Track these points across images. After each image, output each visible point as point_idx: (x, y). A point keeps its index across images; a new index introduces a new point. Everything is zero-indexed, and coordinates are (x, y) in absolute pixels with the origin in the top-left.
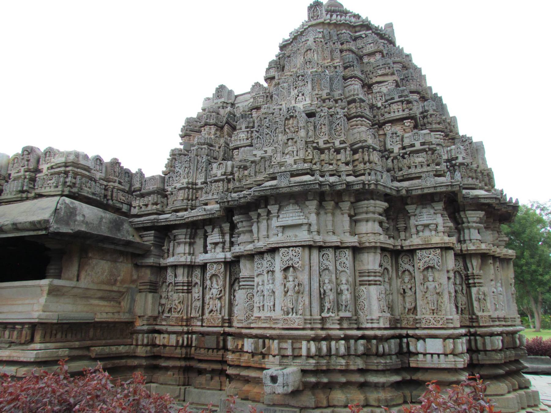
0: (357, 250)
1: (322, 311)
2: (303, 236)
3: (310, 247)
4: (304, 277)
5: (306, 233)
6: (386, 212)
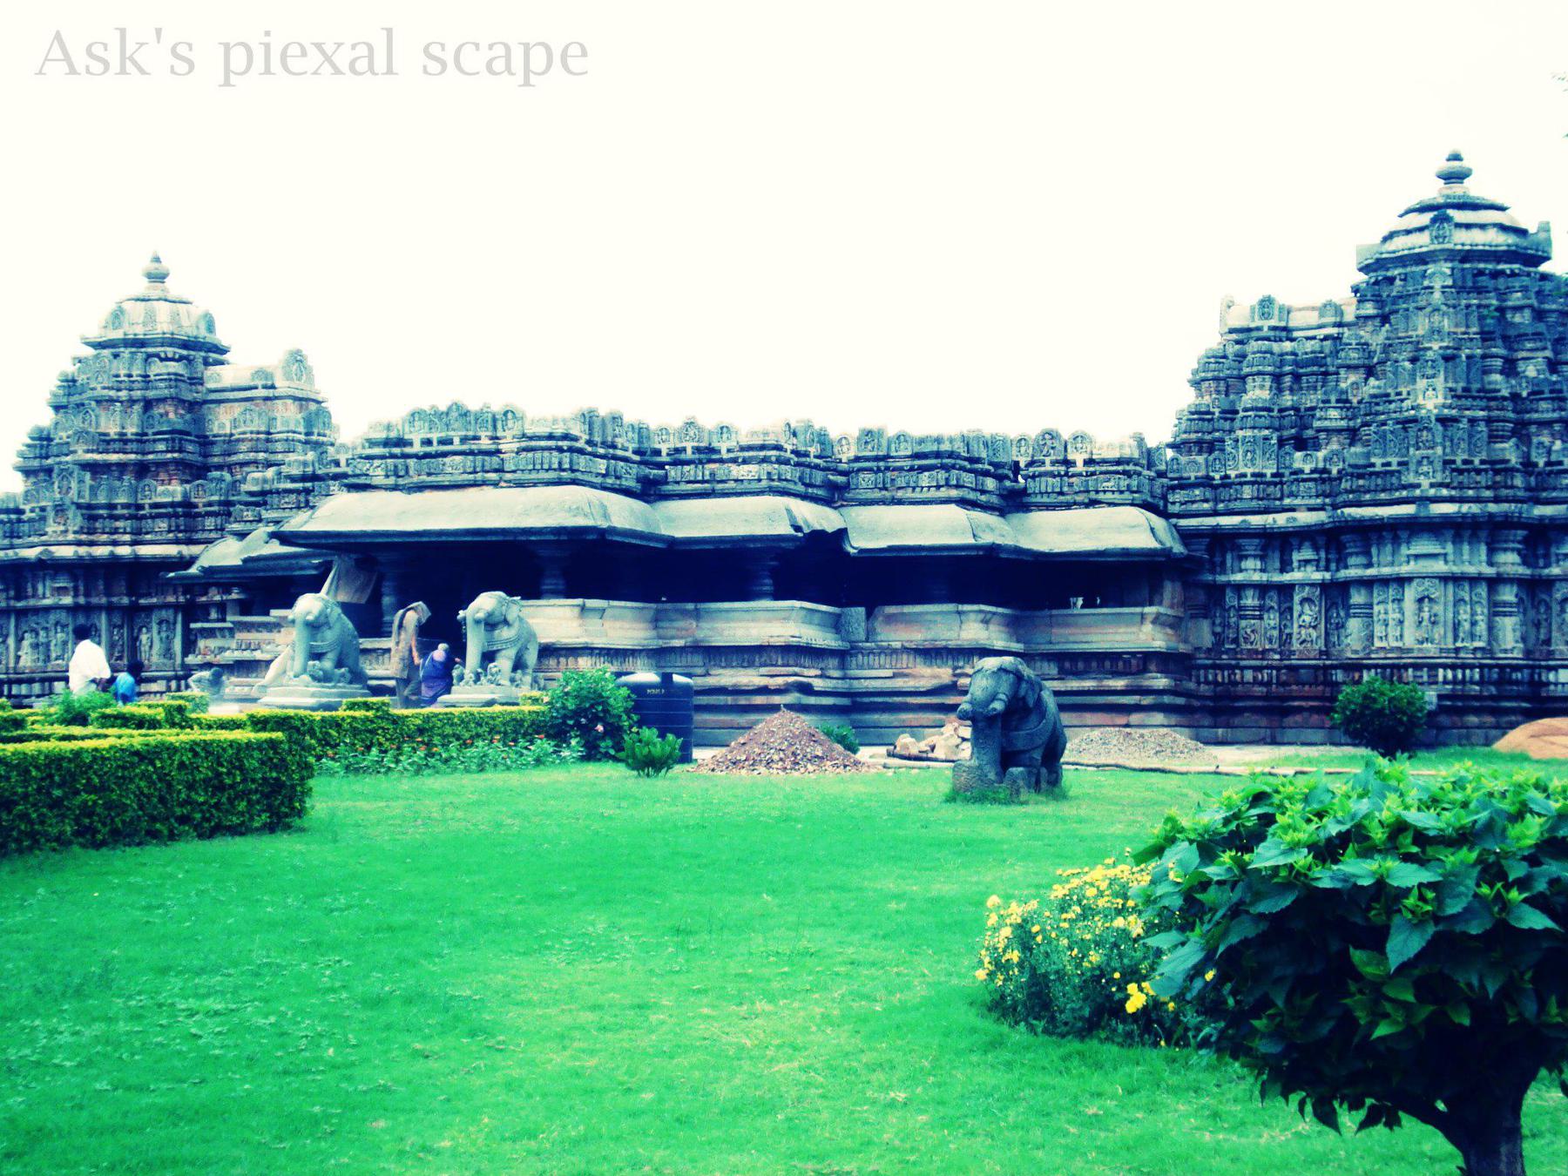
0: (1494, 583)
1: (1455, 640)
2: (1439, 567)
3: (1445, 579)
4: (1438, 609)
5: (1441, 563)
6: (1525, 541)
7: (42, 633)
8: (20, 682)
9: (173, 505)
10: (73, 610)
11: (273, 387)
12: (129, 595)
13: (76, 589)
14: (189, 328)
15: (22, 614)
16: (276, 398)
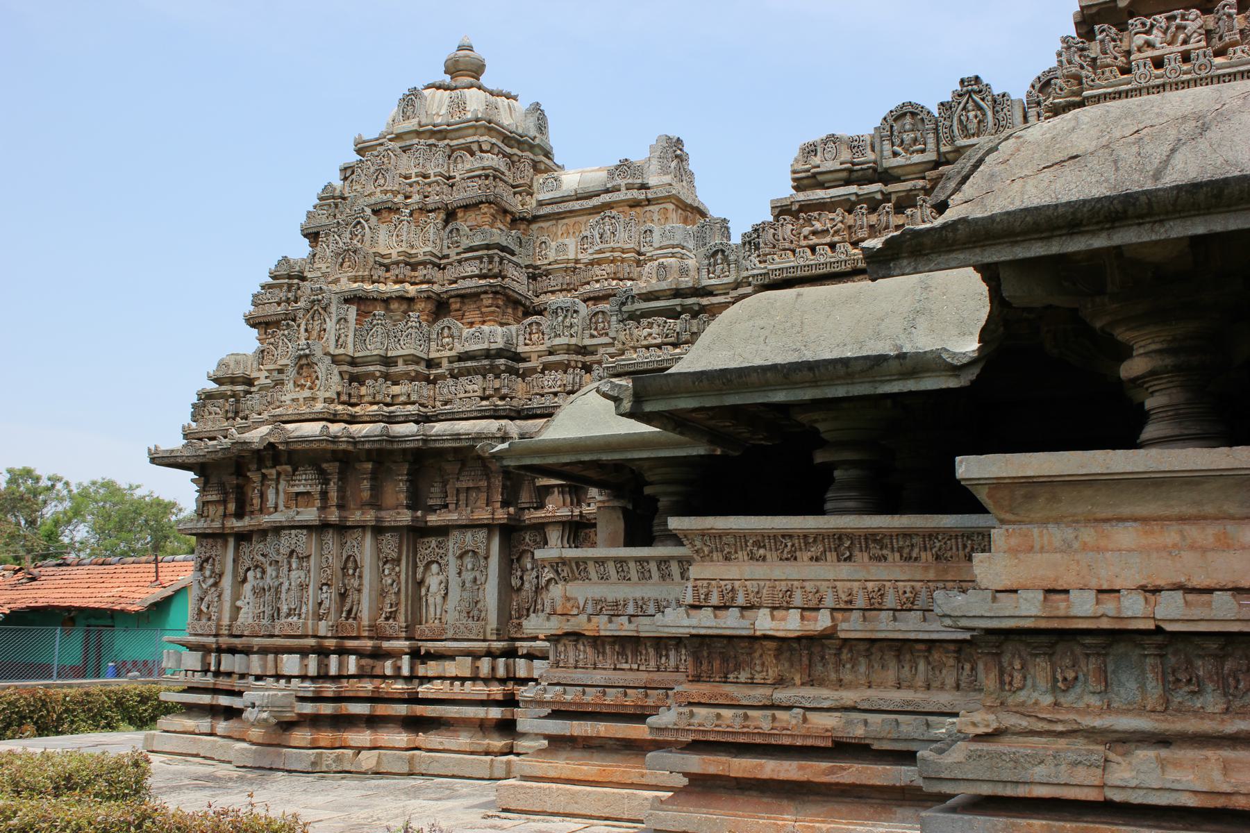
7: (270, 571)
8: (232, 651)
9: (487, 354)
10: (321, 528)
11: (644, 187)
12: (412, 507)
13: (324, 495)
14: (511, 118)
15: (243, 537)
16: (649, 202)
